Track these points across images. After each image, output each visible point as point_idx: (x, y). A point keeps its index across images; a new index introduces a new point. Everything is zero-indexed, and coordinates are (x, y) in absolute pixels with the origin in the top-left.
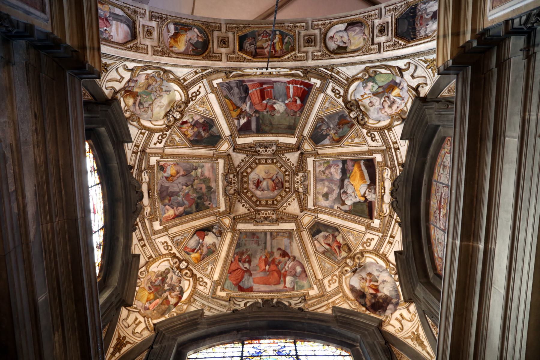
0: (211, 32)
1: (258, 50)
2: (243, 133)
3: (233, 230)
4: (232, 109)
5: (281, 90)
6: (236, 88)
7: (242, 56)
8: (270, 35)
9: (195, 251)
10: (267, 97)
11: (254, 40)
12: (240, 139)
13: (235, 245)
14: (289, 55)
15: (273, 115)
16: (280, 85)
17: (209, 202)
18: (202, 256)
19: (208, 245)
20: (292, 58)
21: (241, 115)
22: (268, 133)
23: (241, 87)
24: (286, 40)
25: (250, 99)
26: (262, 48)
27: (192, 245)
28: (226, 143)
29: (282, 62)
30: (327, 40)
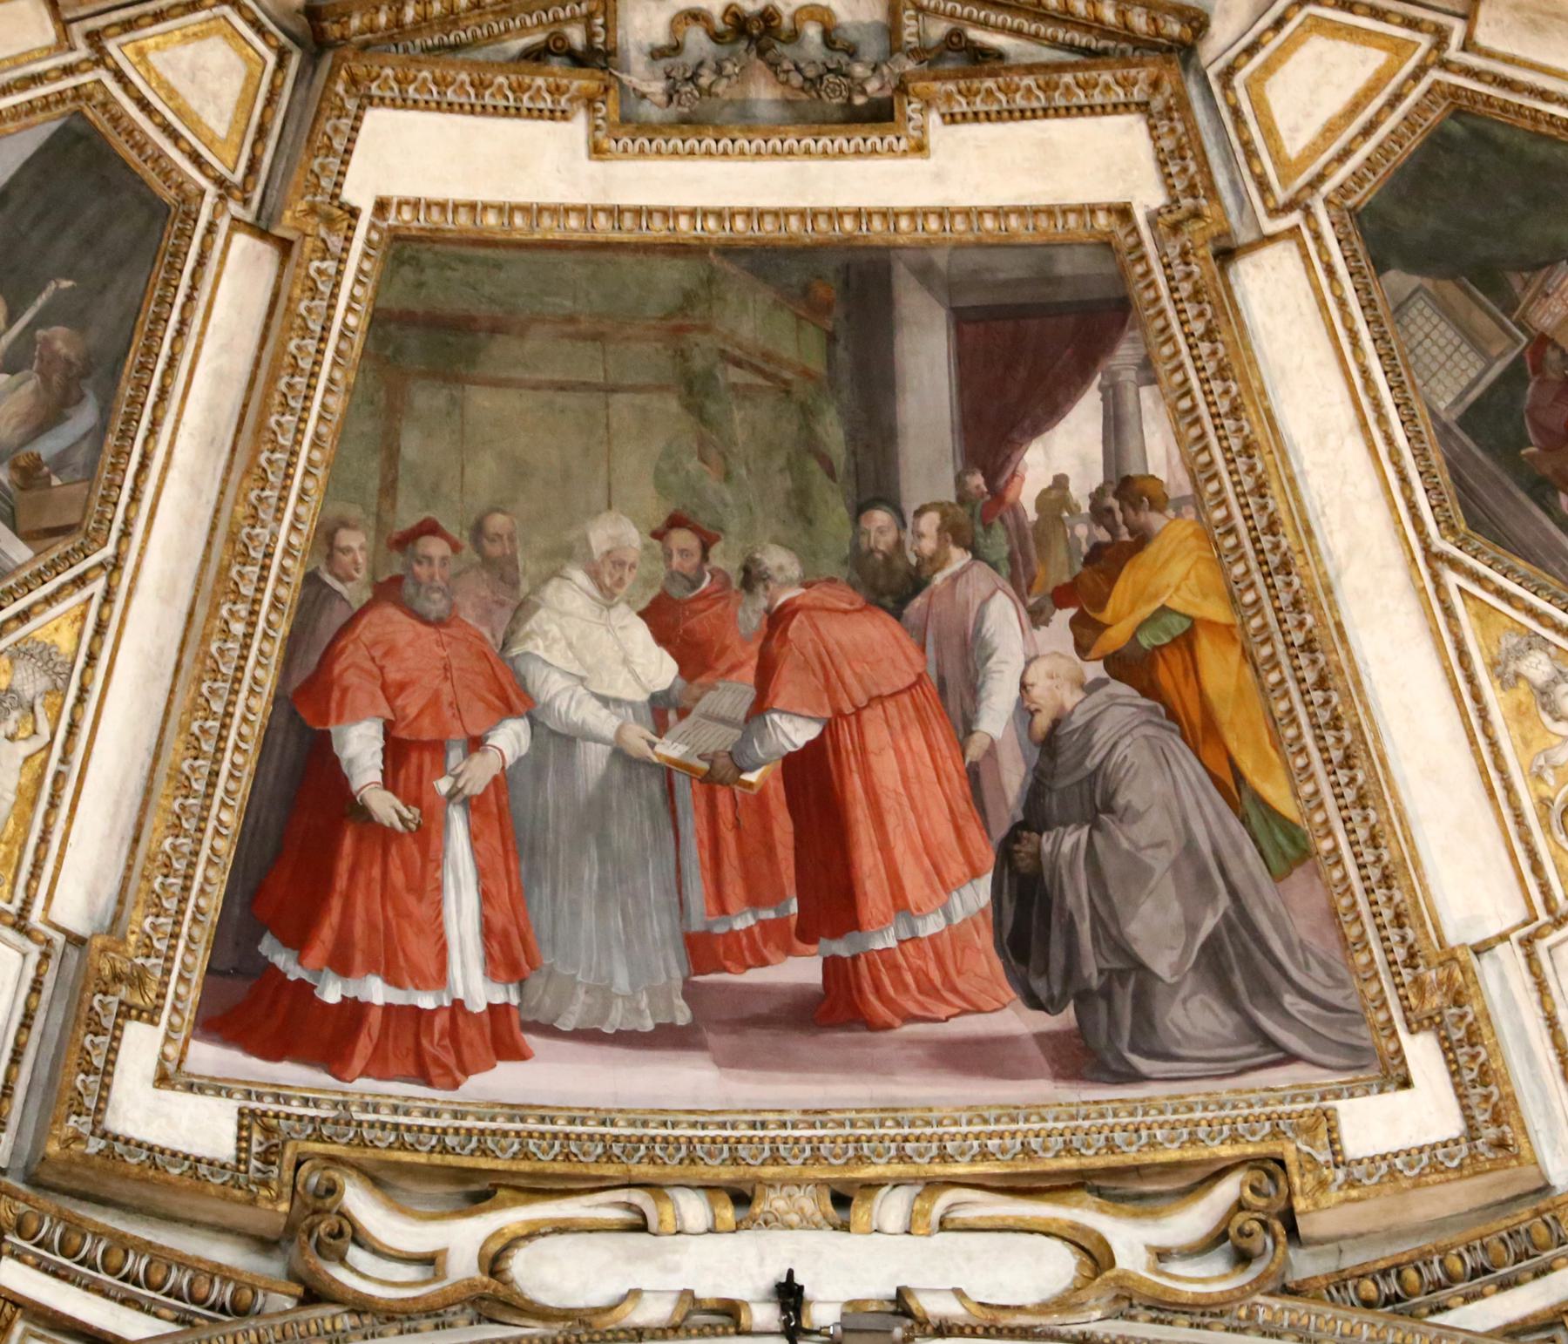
2: (1064, 266)
4: (1206, 647)
5: (588, 917)
6: (1163, 964)
10: (761, 798)
12: (1113, 196)
15: (676, 522)
16: (604, 994)
21: (1097, 551)
22: (729, 250)
23: (1091, 970)
25: (973, 775)
28: (1293, 147)
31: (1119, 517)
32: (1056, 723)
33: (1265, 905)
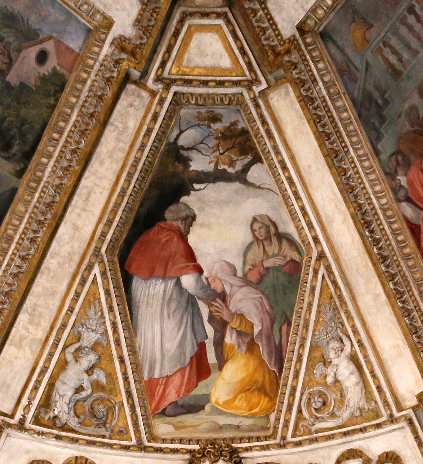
3: (275, 66)
9: (212, 358)
13: (355, 126)
17: (33, 52)
18: (263, 350)
19: (238, 263)
27: (172, 346)
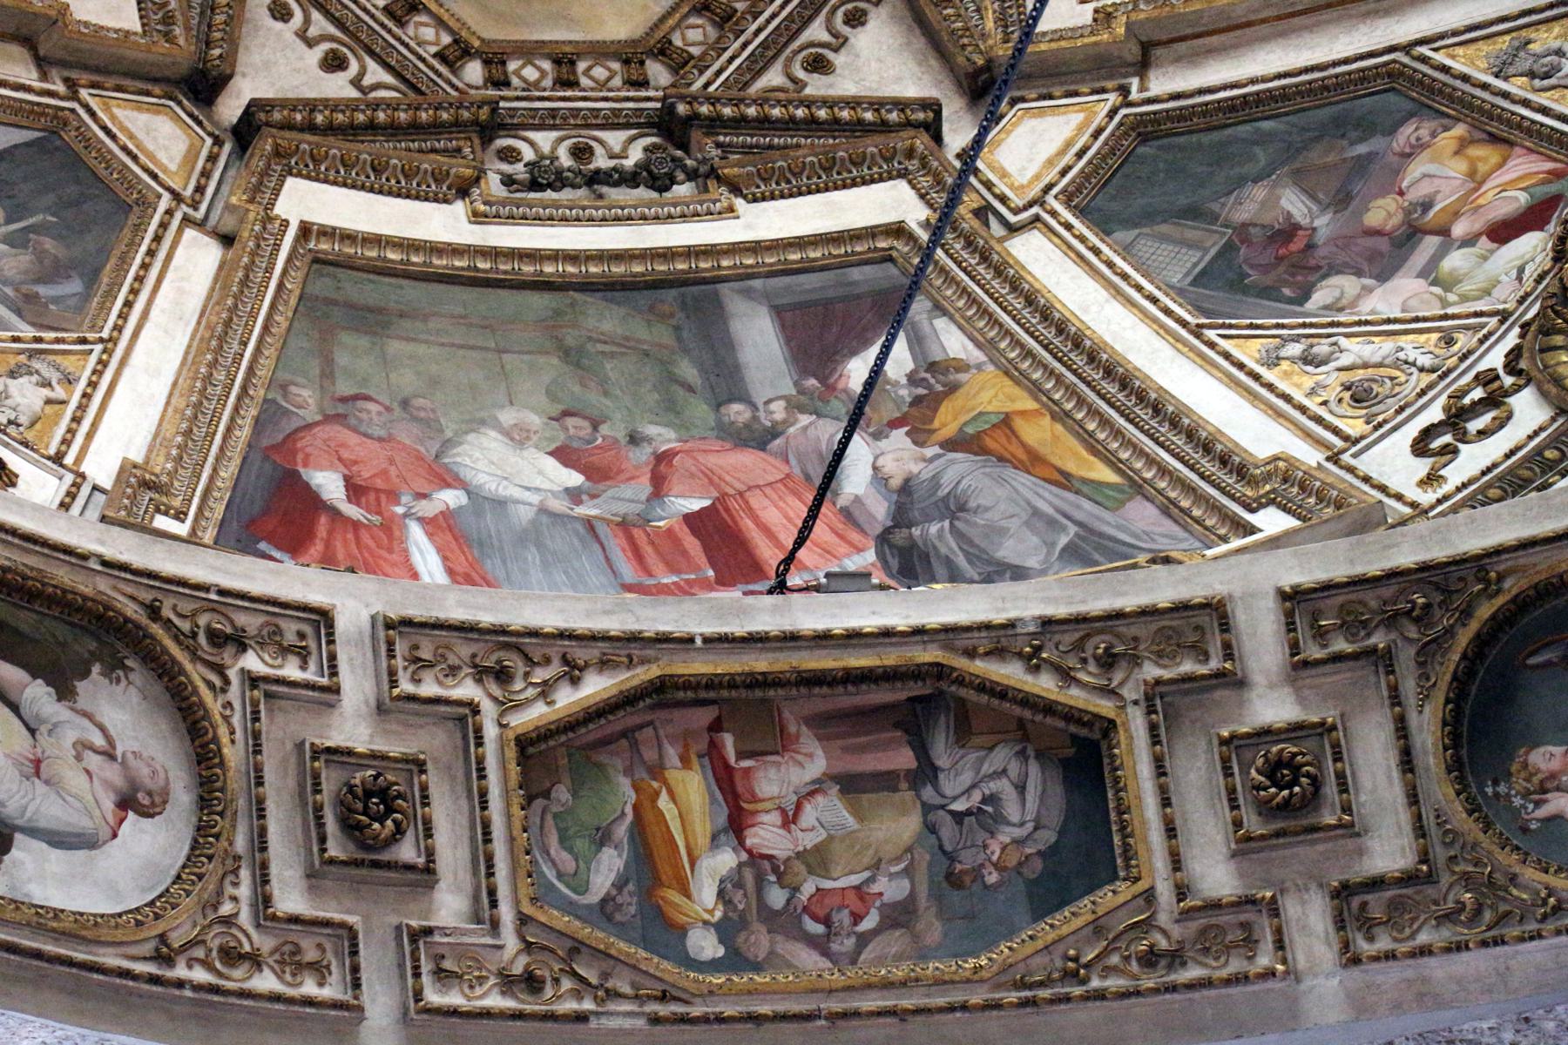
0: (1440, 854)
1: (904, 759)
4: (1019, 424)
7: (1066, 676)
8: (784, 922)
11: (951, 858)
14: (567, 699)
20: (539, 675)
21: (917, 401)
24: (607, 868)
26: (851, 785)
29: (633, 638)
30: (183, 797)
31: (932, 381)
32: (907, 481)
33: (1109, 524)
